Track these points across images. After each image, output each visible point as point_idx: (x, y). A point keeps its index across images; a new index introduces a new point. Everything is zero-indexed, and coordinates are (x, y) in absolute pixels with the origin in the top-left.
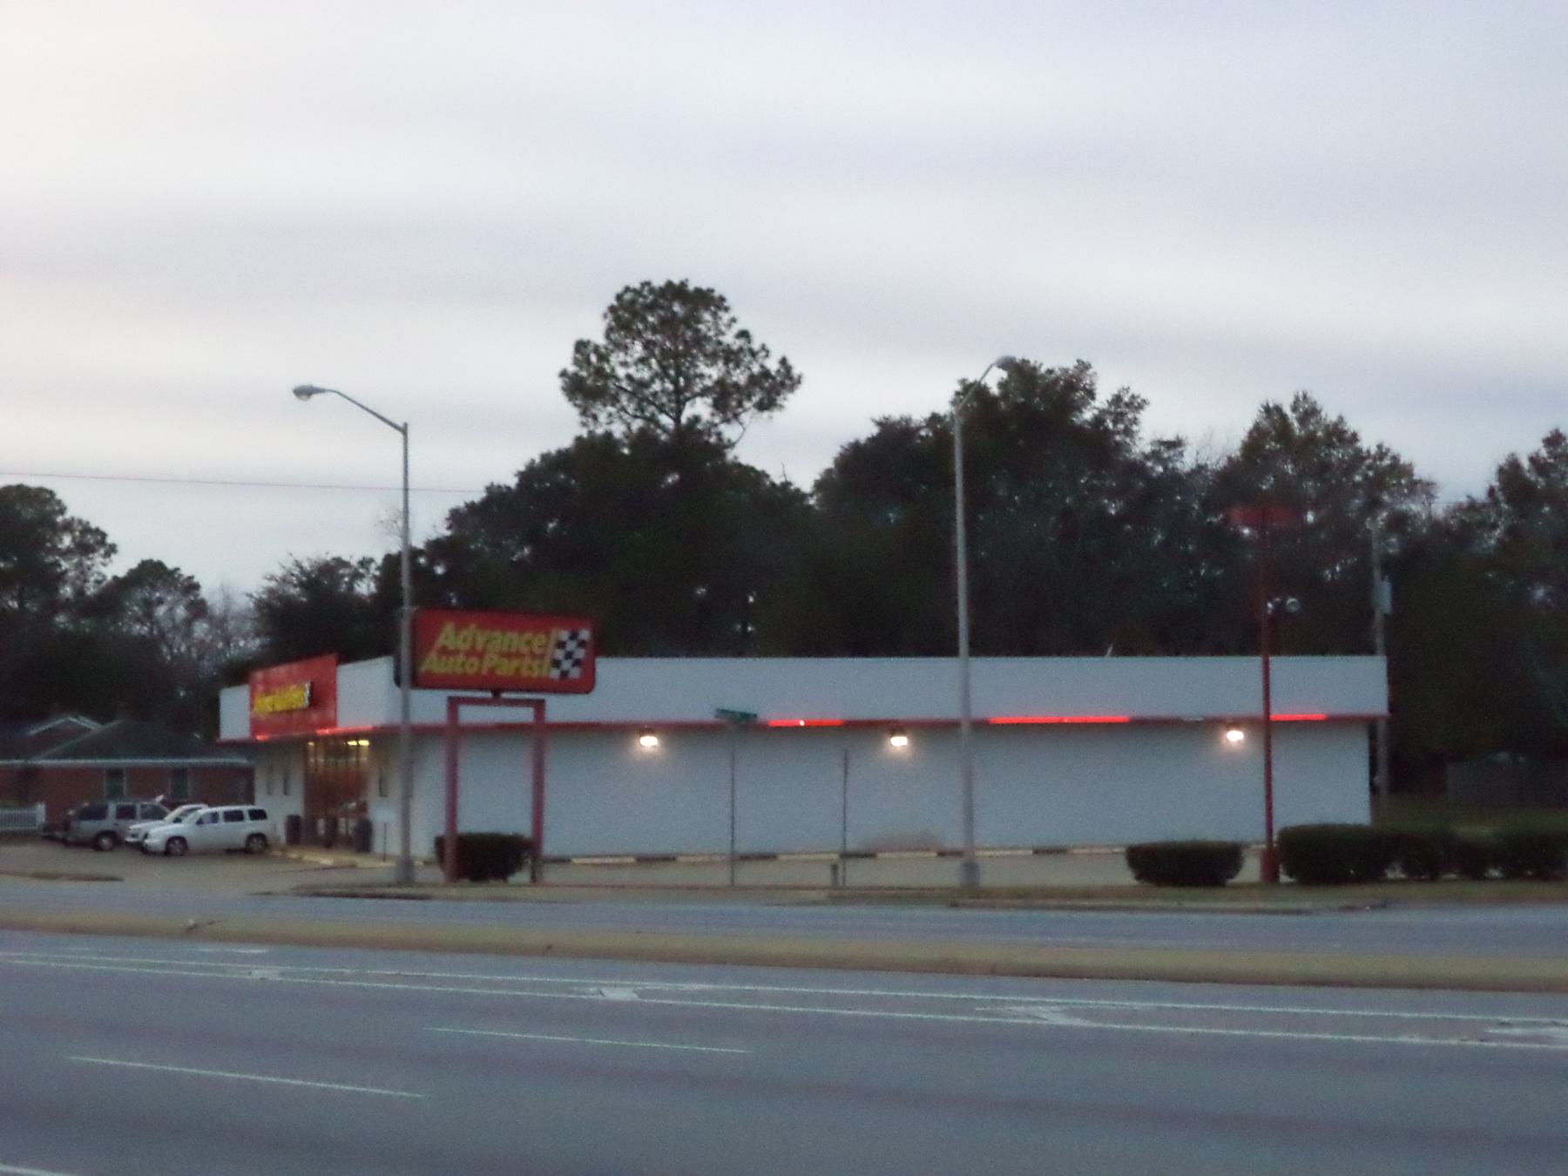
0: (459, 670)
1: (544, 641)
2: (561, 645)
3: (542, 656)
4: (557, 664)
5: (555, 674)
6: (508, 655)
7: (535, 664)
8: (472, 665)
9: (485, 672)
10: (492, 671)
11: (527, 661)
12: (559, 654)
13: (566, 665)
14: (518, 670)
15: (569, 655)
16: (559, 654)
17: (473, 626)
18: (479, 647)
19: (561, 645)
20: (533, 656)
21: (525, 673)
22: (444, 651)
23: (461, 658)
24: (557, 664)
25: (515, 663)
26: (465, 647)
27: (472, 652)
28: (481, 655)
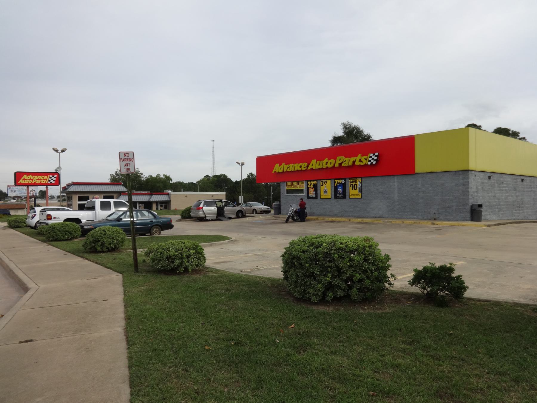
0: (27, 182)
1: (47, 177)
2: (50, 178)
3: (46, 180)
4: (49, 181)
5: (49, 182)
6: (39, 180)
7: (45, 181)
8: (30, 182)
9: (33, 182)
10: (35, 182)
11: (43, 180)
12: (50, 179)
13: (52, 181)
14: (41, 182)
15: (52, 179)
16: (50, 179)
17: (31, 175)
18: (32, 178)
19: (50, 178)
20: (44, 180)
21: (42, 182)
22: (24, 179)
23: (28, 180)
24: (49, 181)
25: (40, 181)
26: (29, 179)
27: (30, 179)
28: (32, 180)
